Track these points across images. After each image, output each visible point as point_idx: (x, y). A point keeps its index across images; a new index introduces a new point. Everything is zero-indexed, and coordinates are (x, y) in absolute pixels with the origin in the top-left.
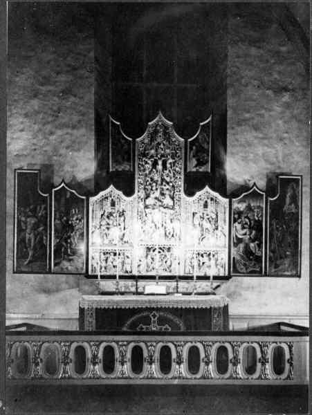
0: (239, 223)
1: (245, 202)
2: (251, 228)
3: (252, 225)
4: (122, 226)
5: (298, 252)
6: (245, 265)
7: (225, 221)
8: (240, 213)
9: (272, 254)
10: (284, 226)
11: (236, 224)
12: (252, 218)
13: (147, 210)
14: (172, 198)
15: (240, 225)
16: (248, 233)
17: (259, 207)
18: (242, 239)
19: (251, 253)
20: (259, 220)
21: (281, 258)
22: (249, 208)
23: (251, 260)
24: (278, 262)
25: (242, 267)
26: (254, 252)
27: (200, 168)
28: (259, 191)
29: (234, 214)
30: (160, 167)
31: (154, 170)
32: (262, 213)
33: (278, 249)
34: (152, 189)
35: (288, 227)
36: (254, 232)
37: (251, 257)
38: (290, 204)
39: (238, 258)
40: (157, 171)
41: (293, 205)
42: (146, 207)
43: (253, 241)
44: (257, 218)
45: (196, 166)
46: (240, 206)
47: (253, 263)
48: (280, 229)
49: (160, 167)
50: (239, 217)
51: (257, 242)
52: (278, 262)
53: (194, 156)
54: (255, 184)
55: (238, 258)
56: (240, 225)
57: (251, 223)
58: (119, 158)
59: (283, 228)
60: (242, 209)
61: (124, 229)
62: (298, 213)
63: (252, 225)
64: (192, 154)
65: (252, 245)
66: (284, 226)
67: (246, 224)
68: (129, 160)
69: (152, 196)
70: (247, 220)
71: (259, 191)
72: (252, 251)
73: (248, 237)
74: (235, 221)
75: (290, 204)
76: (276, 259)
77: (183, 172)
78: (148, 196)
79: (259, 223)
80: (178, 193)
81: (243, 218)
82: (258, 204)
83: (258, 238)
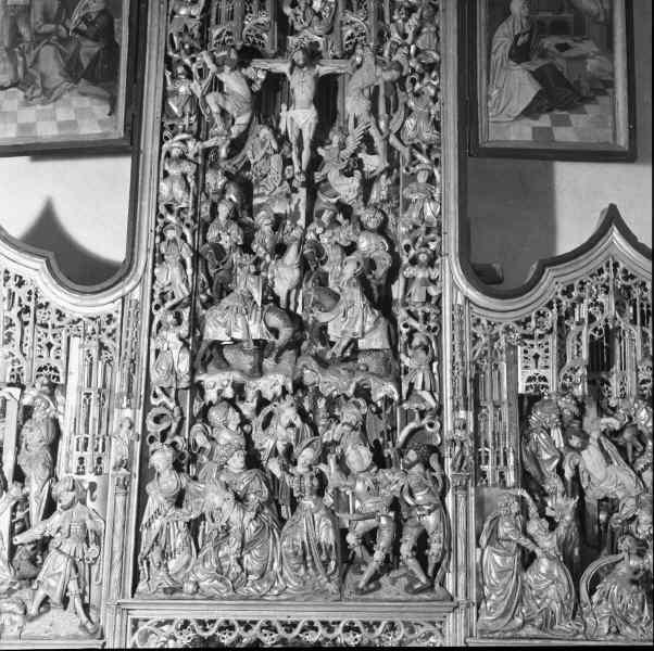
4: (36, 488)
13: (215, 382)
14: (382, 303)
27: (567, 123)
30: (300, 117)
31: (265, 132)
34: (246, 248)
40: (282, 140)
42: (207, 354)
45: (530, 112)
49: (300, 117)
53: (520, 54)
58: (50, 63)
61: (50, 508)
64: (503, 40)
68: (96, 74)
69: (247, 284)
77: (450, 153)
78: (214, 287)
80: (420, 274)
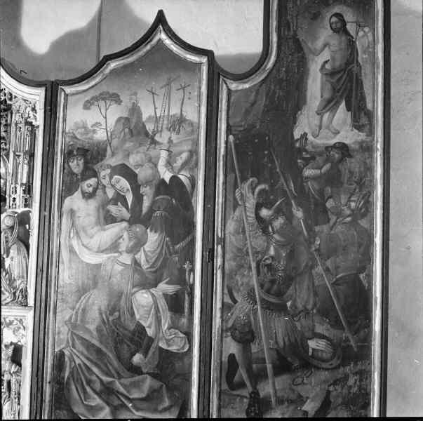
0: (88, 196)
1: (116, 98)
2: (137, 218)
3: (146, 204)
5: (367, 339)
6: (107, 392)
7: (28, 189)
8: (91, 156)
9: (232, 347)
10: (299, 214)
11: (75, 201)
12: (143, 173)
15: (93, 204)
16: (125, 244)
17: (178, 123)
18: (98, 266)
19: (139, 339)
20: (174, 179)
21: (282, 367)
22: (135, 129)
23: (136, 370)
24: (266, 389)
25: (96, 401)
26: (150, 332)
28: (175, 48)
29: (68, 155)
32: (193, 153)
33: (267, 327)
35: (318, 212)
36: (153, 238)
37: (137, 358)
38: (329, 105)
39: (77, 356)
41: (342, 112)
43: (148, 283)
44: (167, 176)
46: (91, 117)
47: (148, 383)
48: (279, 222)
50: (89, 172)
51: (165, 287)
52: (266, 389)
54: (161, 19)
55: (77, 356)
56: (93, 204)
57: (138, 198)
59: (290, 217)
60: (101, 135)
62: (367, 149)
63: (146, 204)
65: (143, 298)
66: (299, 214)
67: (119, 198)
70: (124, 183)
71: (175, 48)
72: (141, 330)
73: (127, 259)
74: (68, 189)
75: (329, 105)
76: (258, 376)
79: (176, 193)
81: (105, 173)
82: (175, 111)
83: (171, 267)
